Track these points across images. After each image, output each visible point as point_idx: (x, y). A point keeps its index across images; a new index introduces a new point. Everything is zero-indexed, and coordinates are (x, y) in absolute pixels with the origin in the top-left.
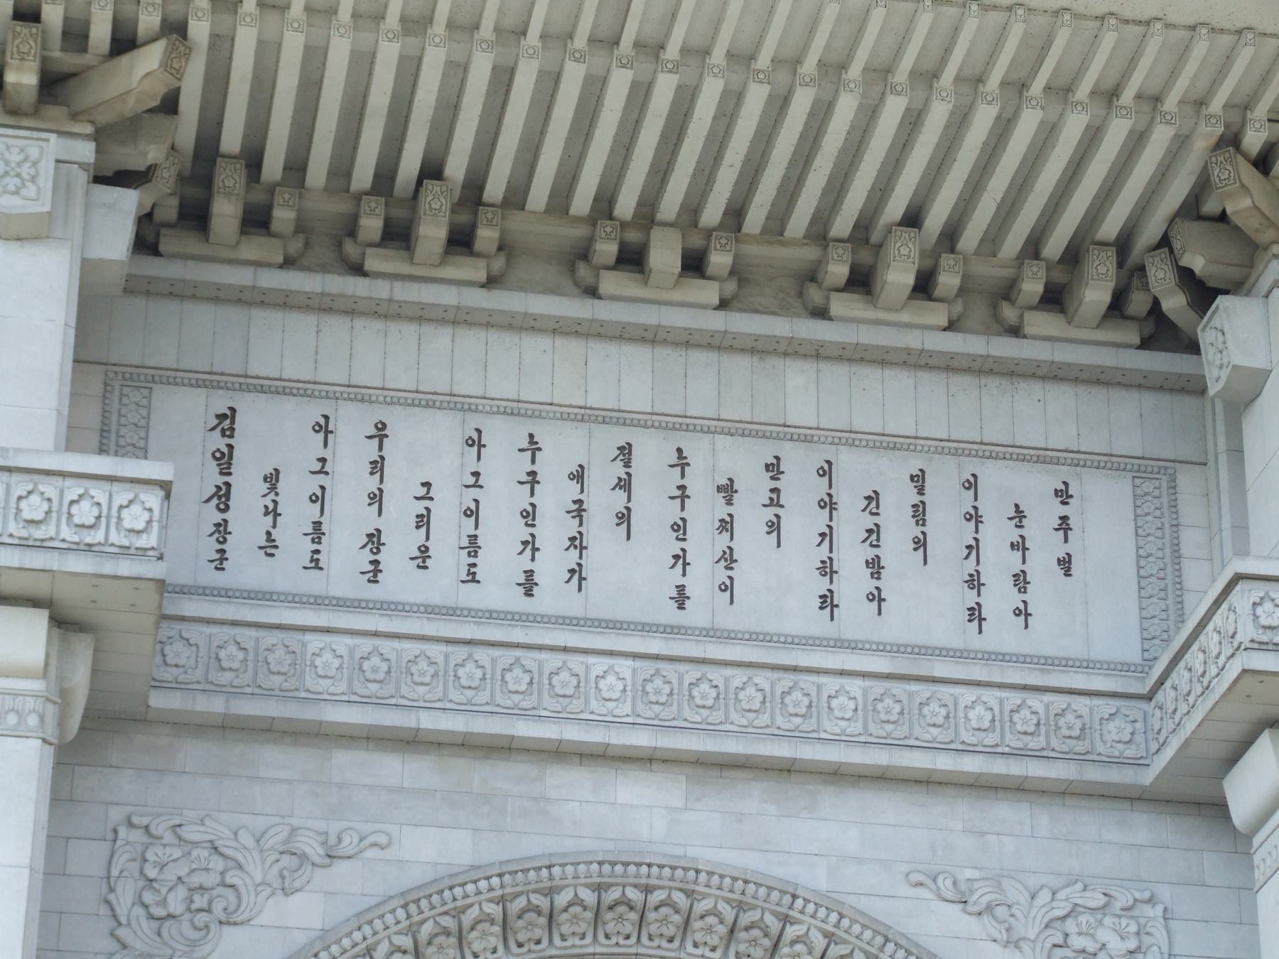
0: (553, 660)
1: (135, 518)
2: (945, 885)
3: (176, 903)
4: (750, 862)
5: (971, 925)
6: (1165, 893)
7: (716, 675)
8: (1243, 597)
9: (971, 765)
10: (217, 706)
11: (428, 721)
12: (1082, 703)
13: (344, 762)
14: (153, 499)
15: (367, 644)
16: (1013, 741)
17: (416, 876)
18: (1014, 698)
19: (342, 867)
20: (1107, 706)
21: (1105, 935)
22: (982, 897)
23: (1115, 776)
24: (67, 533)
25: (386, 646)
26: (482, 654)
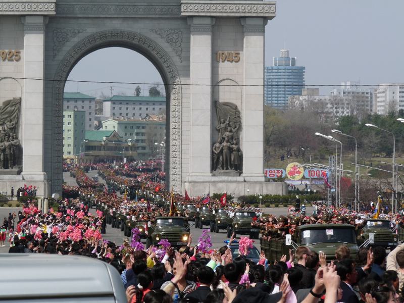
0: (105, 6)
1: (52, 7)
2: (154, 31)
3: (61, 39)
4: (130, 29)
5: (156, 35)
6: (182, 30)
7: (125, 7)
8: (182, 5)
9: (157, 16)
10: (64, 16)
11: (90, 16)
12: (172, 7)
13: (80, 21)
14: (54, 4)
15: (82, 6)
16: (162, 13)
17: (89, 34)
18: (163, 7)
19: (80, 34)
20: (175, 7)
21: (174, 36)
22: (158, 32)
23: (175, 16)
24: (45, 9)
25: (84, 6)
26: (96, 6)
